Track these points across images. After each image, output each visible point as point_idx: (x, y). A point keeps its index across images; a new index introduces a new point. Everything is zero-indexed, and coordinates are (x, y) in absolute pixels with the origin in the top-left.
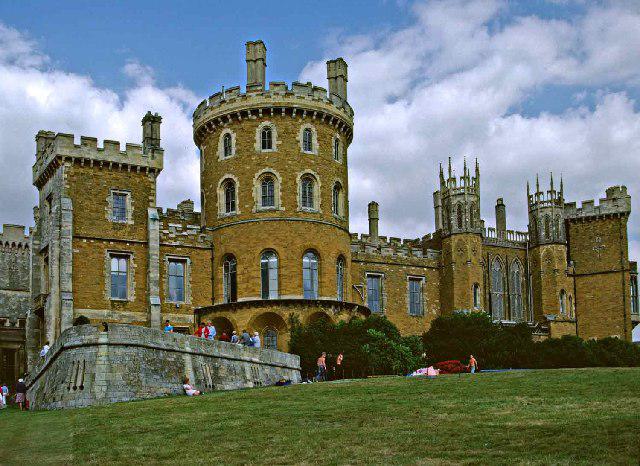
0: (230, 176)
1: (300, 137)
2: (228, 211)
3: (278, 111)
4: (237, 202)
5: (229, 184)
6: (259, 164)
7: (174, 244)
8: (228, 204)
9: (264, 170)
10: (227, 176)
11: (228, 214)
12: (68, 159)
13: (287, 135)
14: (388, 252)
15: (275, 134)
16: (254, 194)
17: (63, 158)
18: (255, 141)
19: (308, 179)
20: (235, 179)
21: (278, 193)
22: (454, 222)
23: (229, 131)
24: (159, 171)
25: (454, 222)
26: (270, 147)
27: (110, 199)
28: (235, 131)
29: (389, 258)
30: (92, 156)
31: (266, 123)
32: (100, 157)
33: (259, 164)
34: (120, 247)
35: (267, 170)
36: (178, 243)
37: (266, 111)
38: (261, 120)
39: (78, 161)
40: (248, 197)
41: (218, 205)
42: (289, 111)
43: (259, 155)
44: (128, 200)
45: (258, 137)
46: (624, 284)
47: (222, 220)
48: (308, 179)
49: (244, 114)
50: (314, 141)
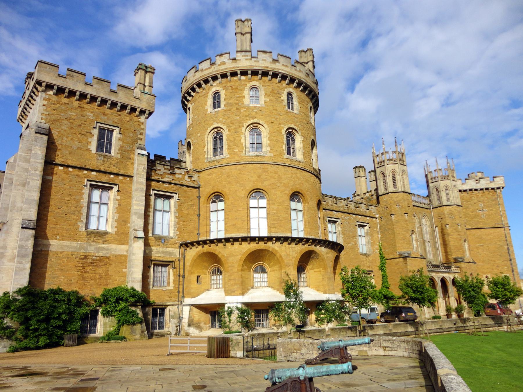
0: (219, 125)
1: (284, 97)
2: (215, 155)
3: (265, 74)
4: (225, 147)
5: (218, 138)
6: (248, 116)
7: (161, 179)
8: (215, 149)
9: (252, 121)
10: (216, 126)
11: (217, 158)
12: (50, 87)
13: (274, 94)
14: (341, 204)
15: (262, 92)
16: (243, 140)
17: (44, 84)
18: (244, 97)
19: (290, 133)
20: (224, 127)
21: (265, 140)
22: (390, 184)
23: (218, 89)
24: (150, 113)
25: (390, 184)
26: (258, 102)
27: (96, 132)
28: (224, 88)
29: (343, 207)
30: (79, 87)
31: (254, 83)
32: (90, 91)
33: (248, 116)
34: (104, 178)
35: (255, 121)
36: (165, 180)
37: (255, 73)
38: (250, 80)
39: (60, 91)
40: (235, 143)
41: (205, 150)
42: (275, 75)
43: (248, 108)
44: (115, 135)
45: (246, 93)
46: (506, 237)
47: (210, 162)
48: (290, 133)
49: (234, 74)
50: (296, 102)
